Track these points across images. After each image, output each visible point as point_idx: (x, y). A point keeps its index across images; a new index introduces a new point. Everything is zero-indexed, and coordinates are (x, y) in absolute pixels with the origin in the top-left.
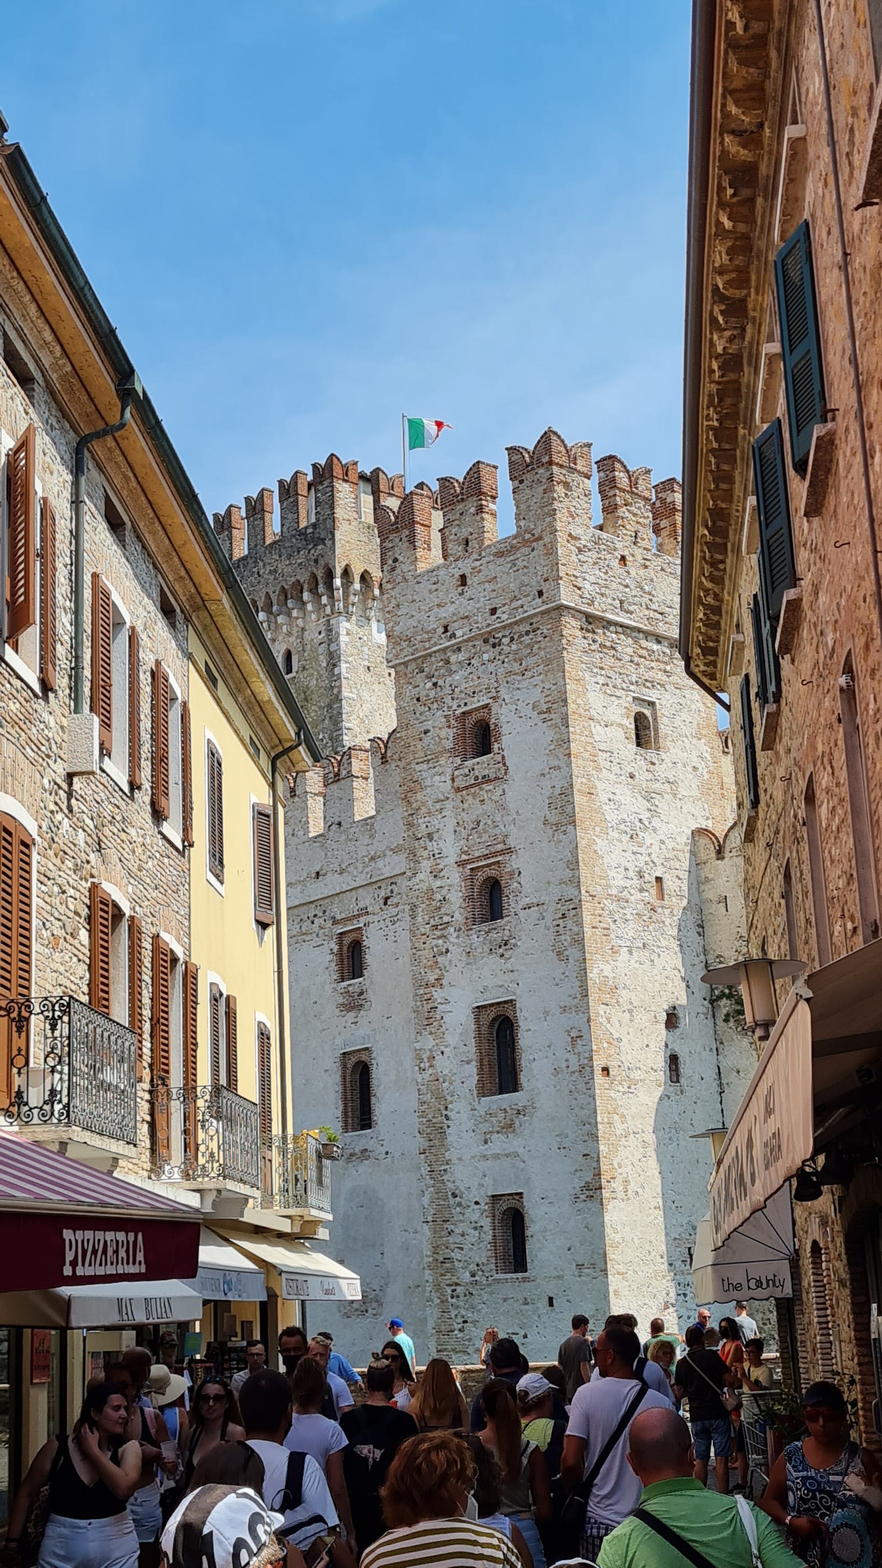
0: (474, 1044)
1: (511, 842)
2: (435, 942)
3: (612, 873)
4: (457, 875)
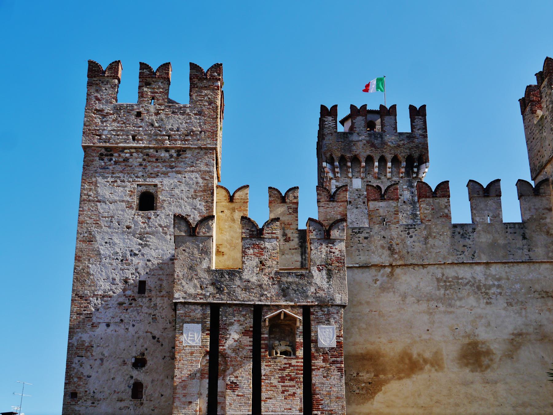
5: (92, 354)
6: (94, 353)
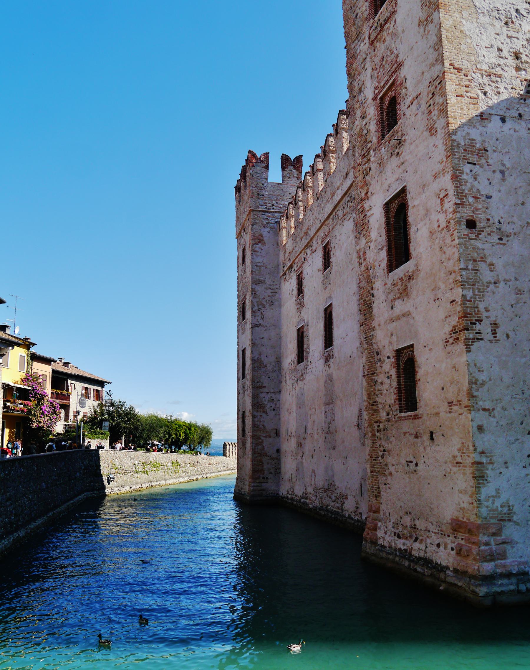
0: (385, 233)
1: (400, 59)
2: (364, 167)
5: (487, 162)
6: (491, 162)
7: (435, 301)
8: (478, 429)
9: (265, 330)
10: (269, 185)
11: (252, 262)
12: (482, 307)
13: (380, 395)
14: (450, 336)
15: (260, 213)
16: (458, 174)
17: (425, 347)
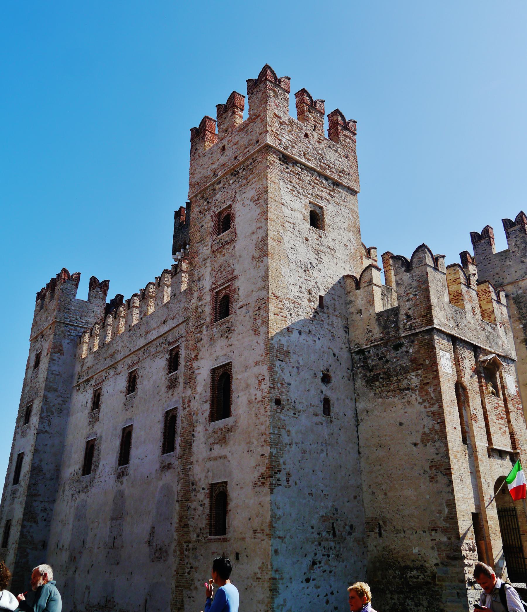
0: (209, 391)
2: (196, 336)
3: (291, 287)
4: (209, 297)
5: (290, 360)
7: (248, 451)
8: (275, 552)
9: (50, 437)
10: (76, 301)
11: (48, 369)
12: (281, 461)
13: (191, 520)
14: (258, 480)
15: (63, 325)
16: (272, 367)
17: (237, 485)
